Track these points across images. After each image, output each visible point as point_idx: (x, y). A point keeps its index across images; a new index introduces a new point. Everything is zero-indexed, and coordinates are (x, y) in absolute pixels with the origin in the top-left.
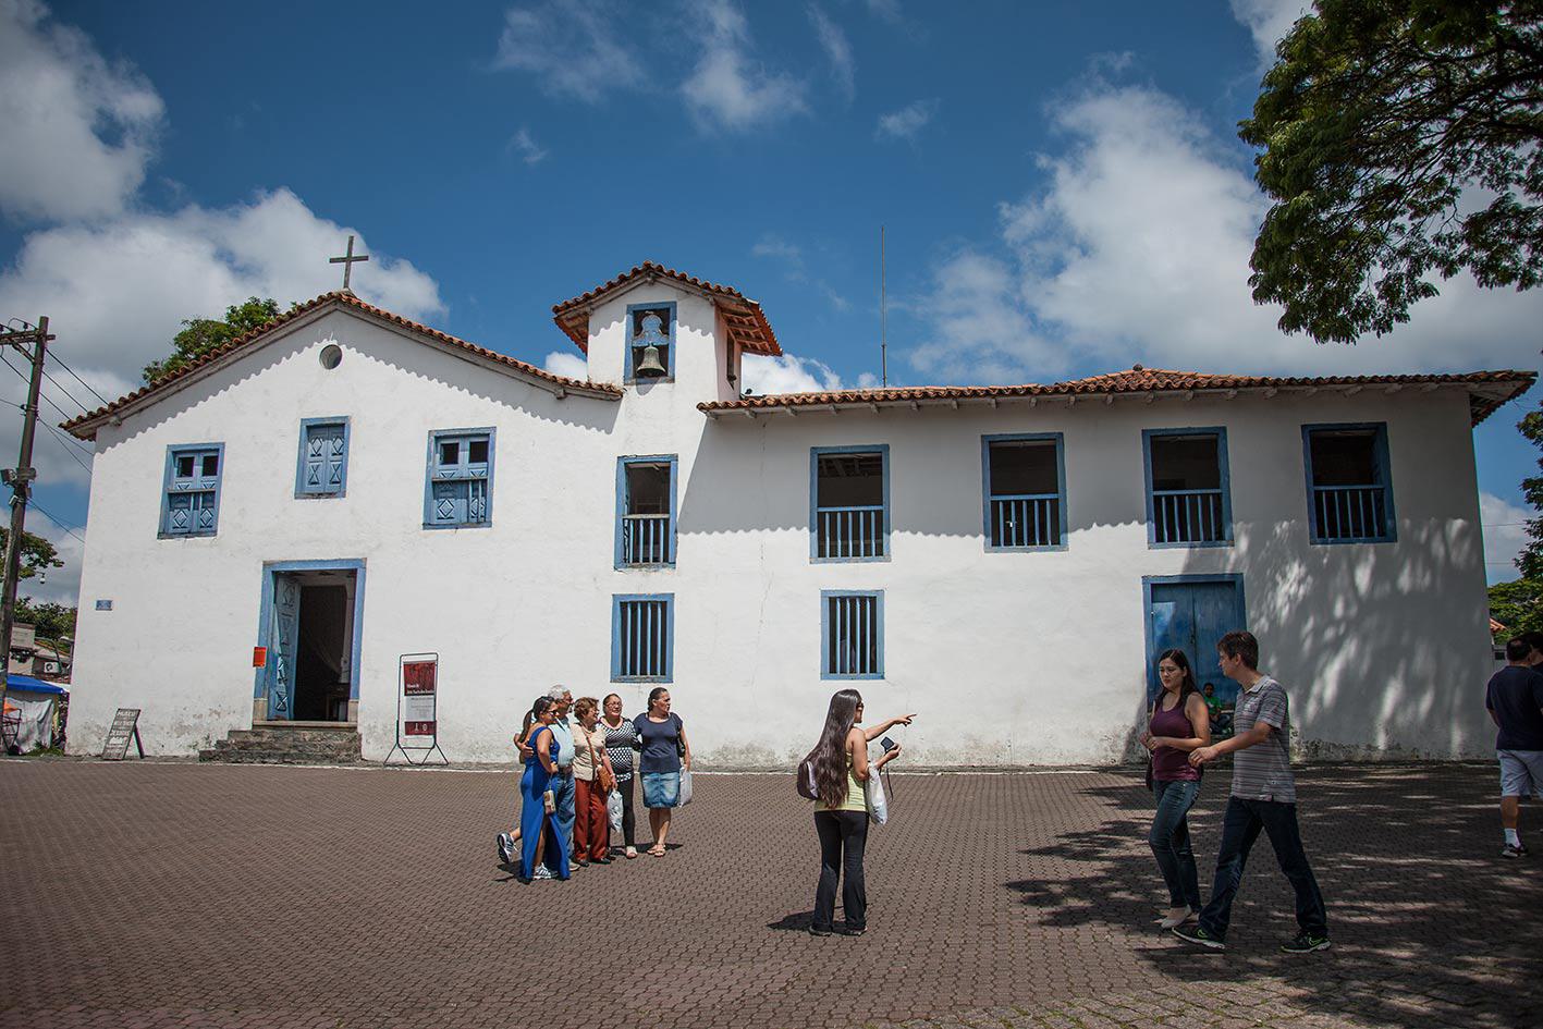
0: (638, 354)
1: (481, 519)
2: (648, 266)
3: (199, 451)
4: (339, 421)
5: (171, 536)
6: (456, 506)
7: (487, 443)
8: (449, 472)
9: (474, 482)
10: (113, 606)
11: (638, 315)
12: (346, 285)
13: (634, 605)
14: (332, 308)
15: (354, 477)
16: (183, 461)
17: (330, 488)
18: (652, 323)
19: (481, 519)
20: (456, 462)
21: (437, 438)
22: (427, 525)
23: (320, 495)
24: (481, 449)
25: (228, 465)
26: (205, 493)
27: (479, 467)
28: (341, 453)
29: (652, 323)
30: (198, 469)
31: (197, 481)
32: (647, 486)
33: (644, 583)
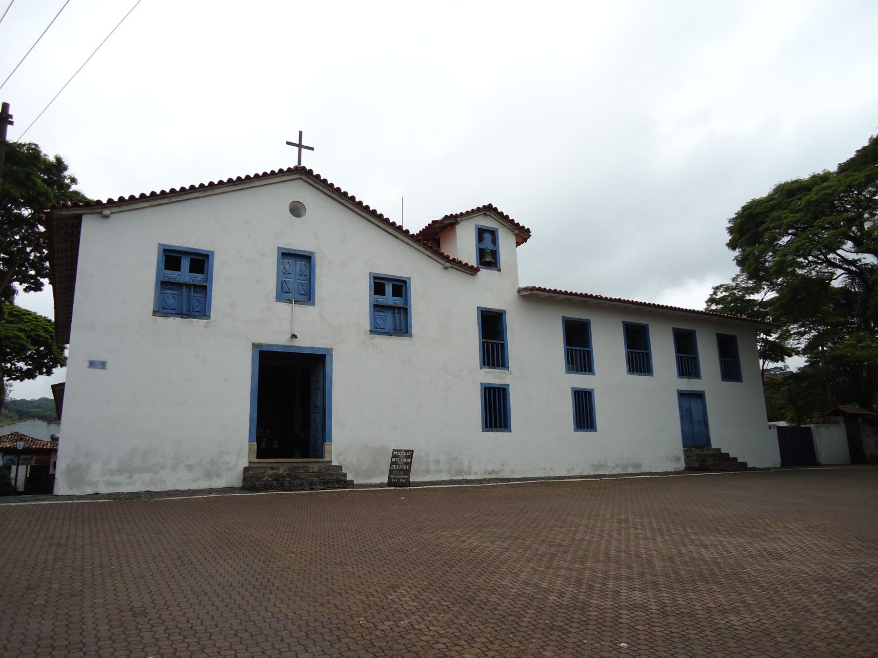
0: (481, 253)
2: (490, 205)
4: (307, 254)
5: (167, 315)
8: (381, 300)
9: (399, 308)
10: (108, 366)
11: (481, 233)
16: (171, 258)
18: (487, 237)
22: (371, 332)
24: (400, 287)
26: (195, 286)
30: (185, 263)
33: (494, 377)
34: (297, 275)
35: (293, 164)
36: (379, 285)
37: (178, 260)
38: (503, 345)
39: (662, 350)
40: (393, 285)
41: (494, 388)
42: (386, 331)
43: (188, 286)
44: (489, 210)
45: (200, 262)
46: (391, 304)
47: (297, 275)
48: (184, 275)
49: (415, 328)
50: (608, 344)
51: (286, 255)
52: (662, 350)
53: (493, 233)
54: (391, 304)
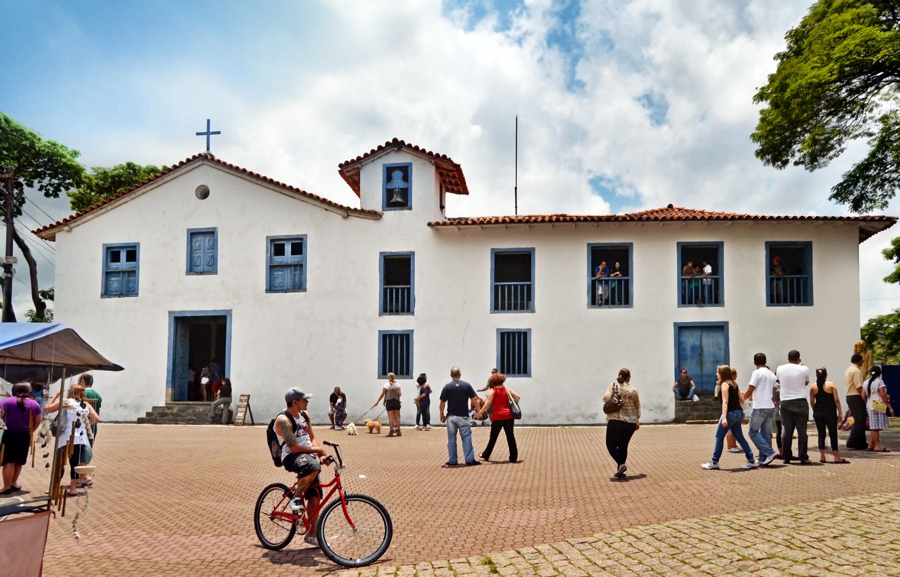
0: (389, 193)
1: (299, 286)
2: (395, 140)
3: (123, 247)
6: (285, 277)
7: (301, 244)
9: (295, 266)
11: (389, 171)
12: (208, 149)
13: (391, 336)
14: (201, 162)
15: (222, 262)
16: (112, 253)
17: (207, 268)
18: (398, 175)
19: (299, 286)
20: (283, 254)
21: (272, 241)
23: (201, 273)
24: (298, 247)
25: (142, 255)
27: (297, 258)
28: (214, 247)
29: (398, 175)
30: (123, 255)
31: (123, 264)
32: (397, 272)
33: (396, 323)
34: (202, 250)
35: (203, 151)
36: (277, 246)
37: (119, 253)
38: (409, 289)
39: (655, 270)
40: (292, 244)
41: (396, 336)
42: (285, 288)
43: (124, 272)
44: (397, 145)
45: (132, 254)
46: (287, 262)
47: (202, 250)
48: (123, 264)
49: (309, 285)
50: (561, 274)
51: (193, 234)
52: (655, 270)
53: (405, 171)
54: (287, 262)
